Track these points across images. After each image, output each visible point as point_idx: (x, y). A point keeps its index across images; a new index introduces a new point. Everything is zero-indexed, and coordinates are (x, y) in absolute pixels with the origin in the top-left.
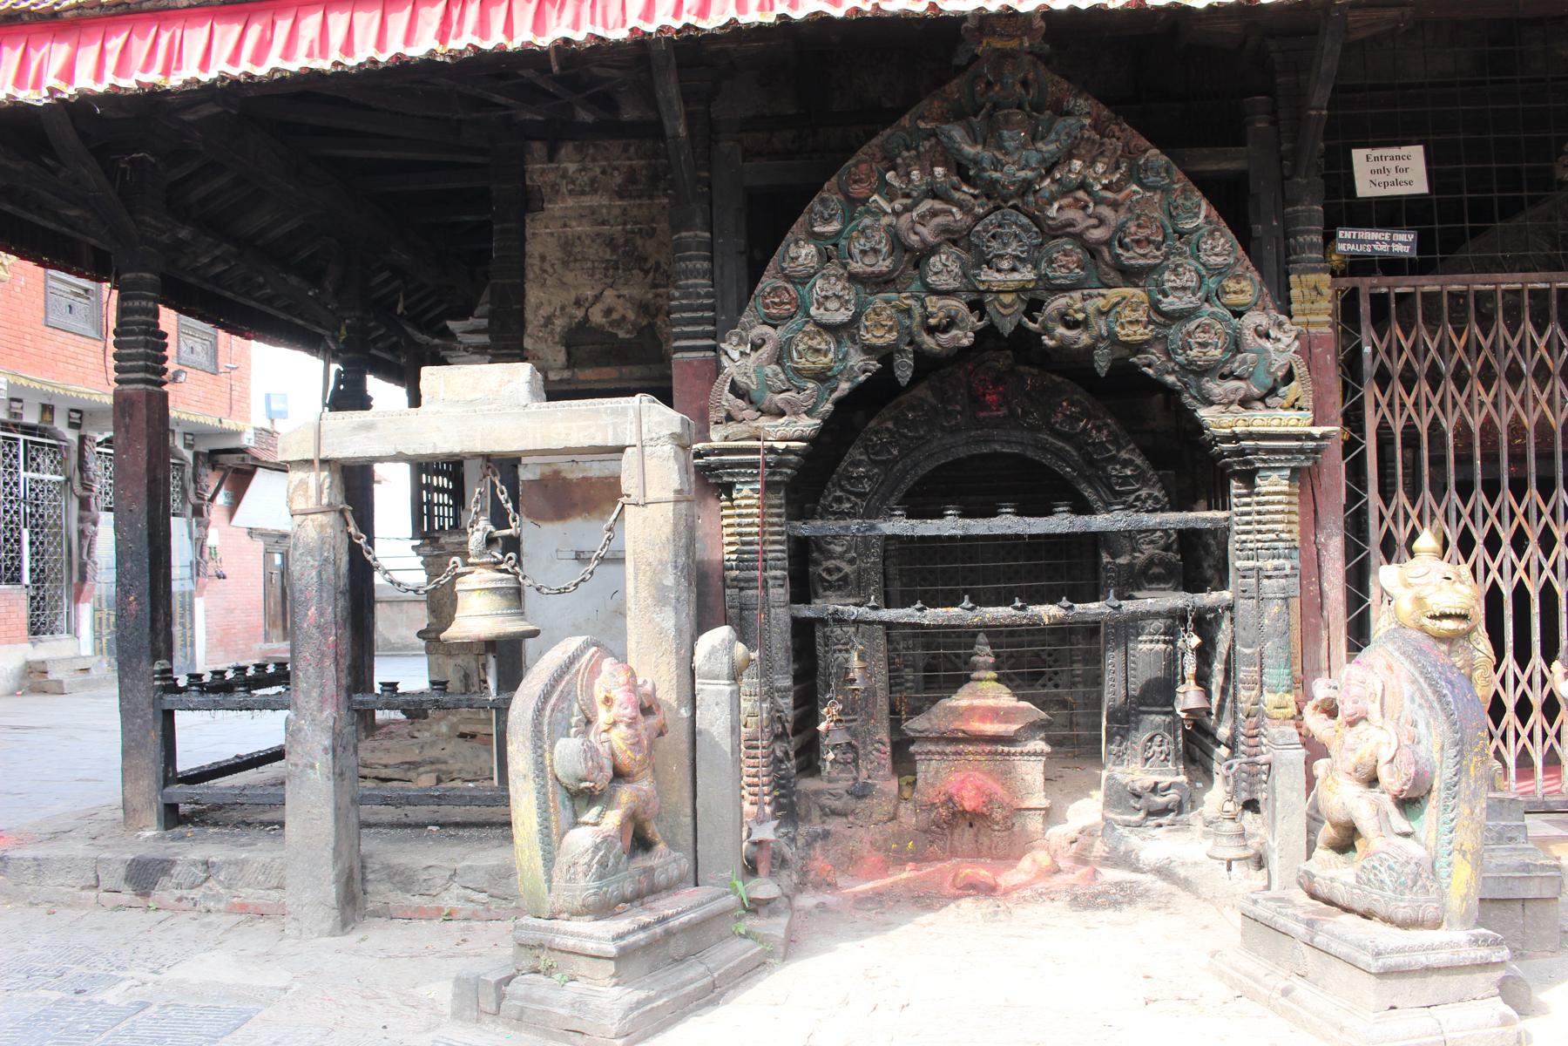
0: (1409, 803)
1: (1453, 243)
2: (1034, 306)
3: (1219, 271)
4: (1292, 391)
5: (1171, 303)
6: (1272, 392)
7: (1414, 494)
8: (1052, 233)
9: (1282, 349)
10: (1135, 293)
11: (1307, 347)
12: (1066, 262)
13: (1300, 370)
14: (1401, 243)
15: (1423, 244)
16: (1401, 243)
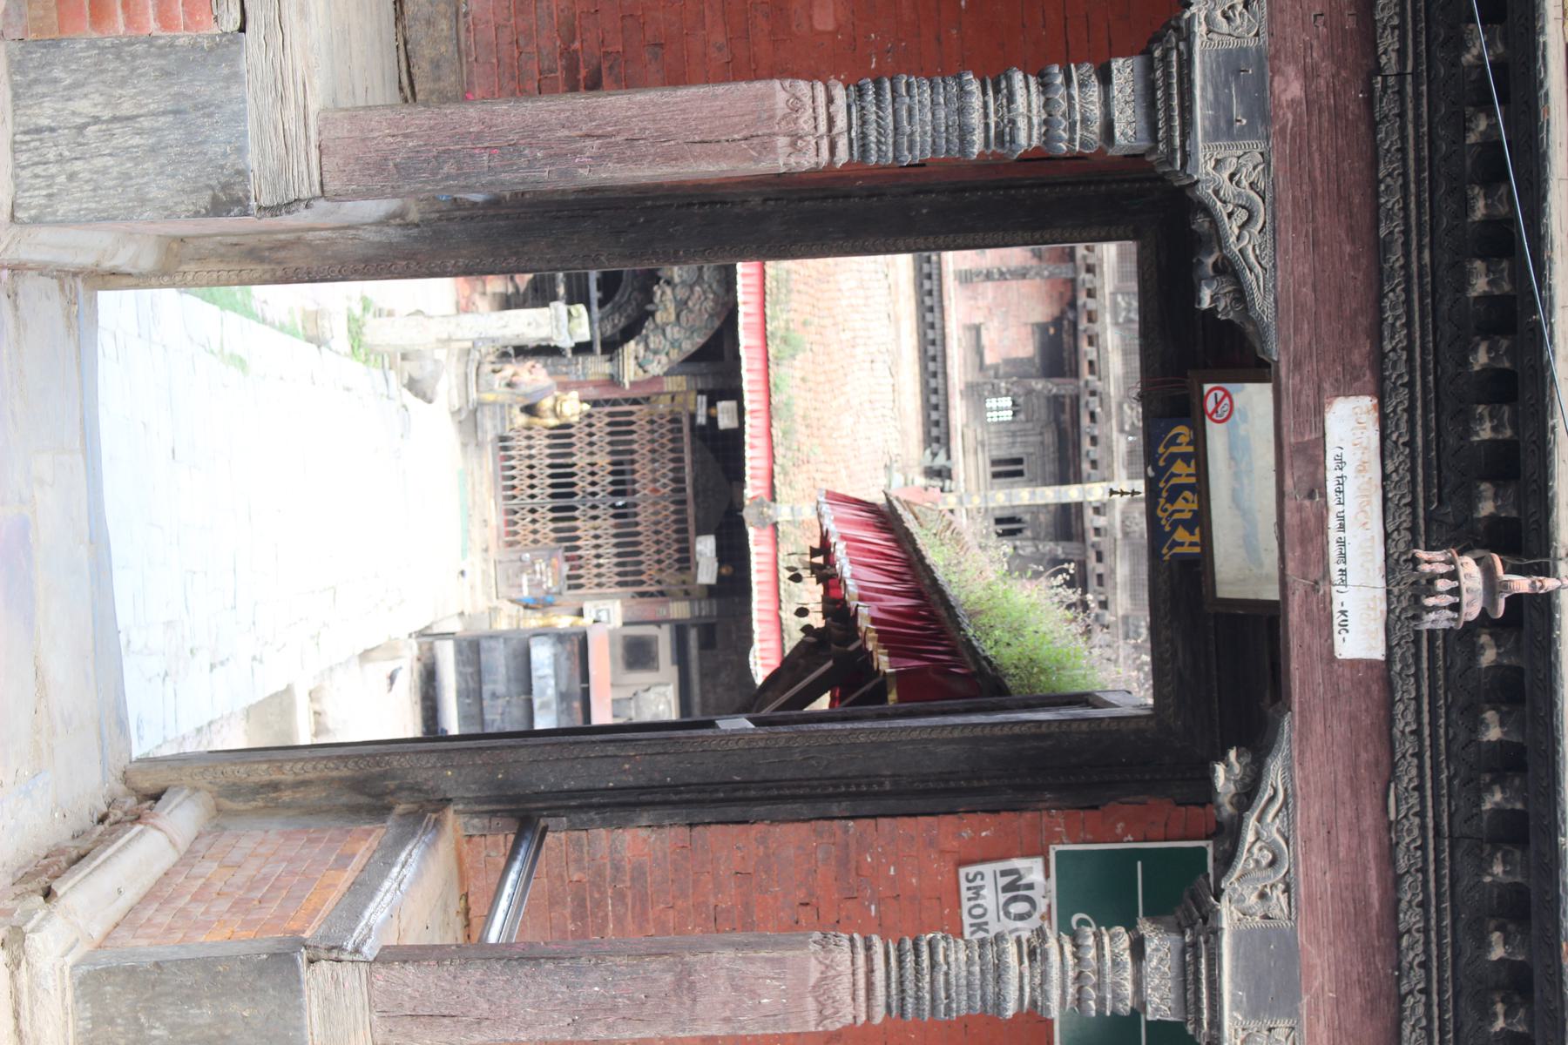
0: (510, 385)
1: (703, 438)
2: (668, 282)
3: (680, 347)
4: (640, 372)
5: (668, 330)
6: (640, 366)
7: (609, 424)
8: (691, 288)
9: (655, 369)
10: (673, 317)
11: (656, 378)
12: (682, 293)
13: (648, 376)
14: (701, 420)
15: (702, 428)
16: (701, 420)
